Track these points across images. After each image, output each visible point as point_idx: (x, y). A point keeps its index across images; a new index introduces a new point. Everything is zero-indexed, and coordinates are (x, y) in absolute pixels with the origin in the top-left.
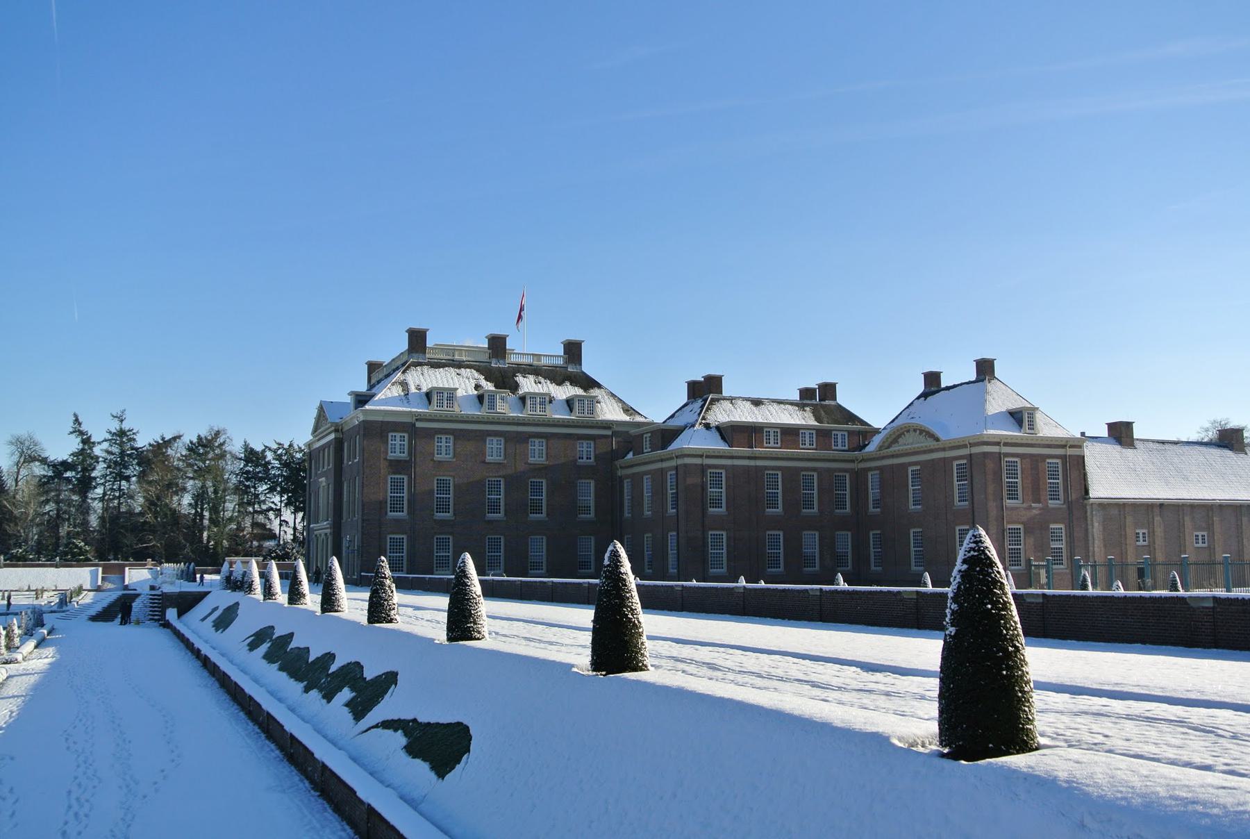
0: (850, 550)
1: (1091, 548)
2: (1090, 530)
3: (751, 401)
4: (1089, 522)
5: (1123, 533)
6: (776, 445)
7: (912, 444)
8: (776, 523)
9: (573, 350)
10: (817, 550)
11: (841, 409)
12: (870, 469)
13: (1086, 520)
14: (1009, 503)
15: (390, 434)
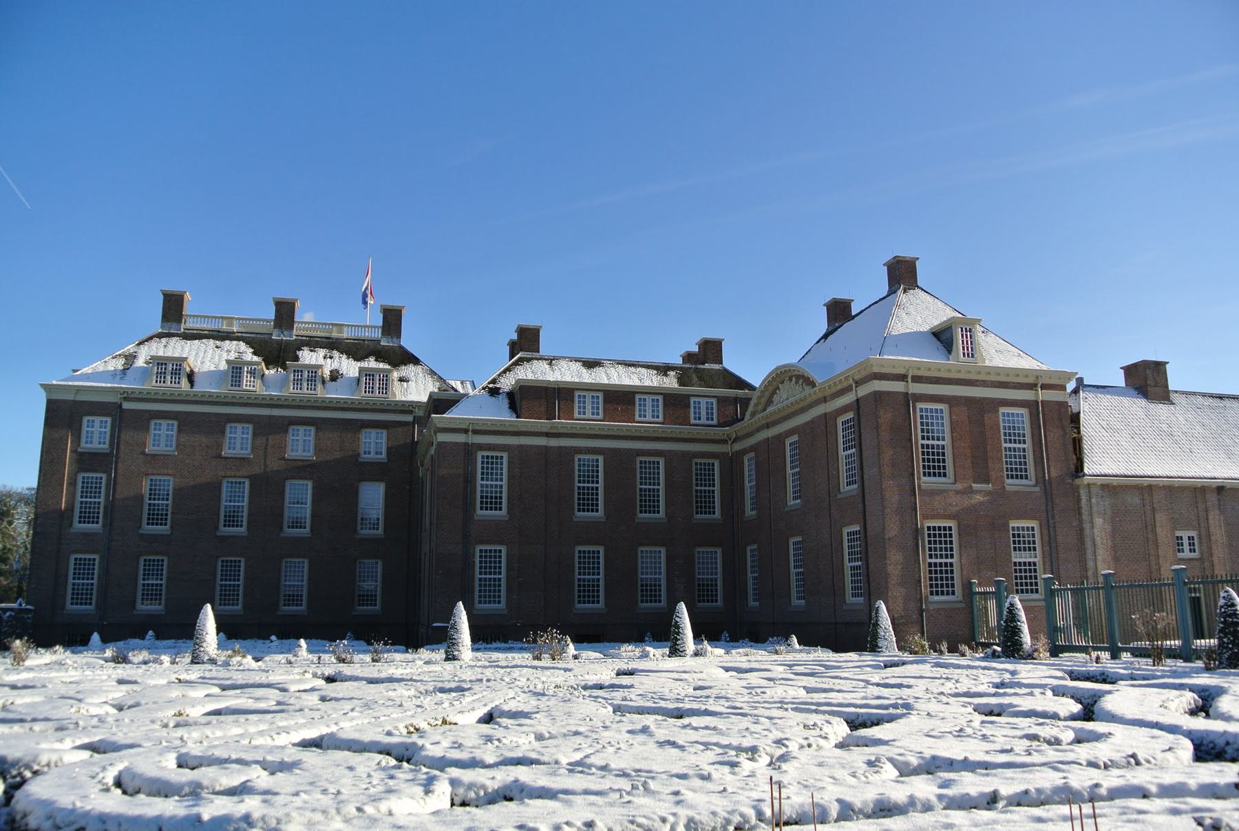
0: (719, 576)
1: (1090, 564)
2: (1087, 532)
3: (583, 362)
4: (1085, 517)
5: (1150, 536)
6: (595, 417)
7: (788, 399)
8: (591, 533)
9: (392, 320)
10: (663, 576)
11: (726, 372)
12: (744, 452)
13: (1080, 514)
14: (927, 482)
15: (85, 419)
